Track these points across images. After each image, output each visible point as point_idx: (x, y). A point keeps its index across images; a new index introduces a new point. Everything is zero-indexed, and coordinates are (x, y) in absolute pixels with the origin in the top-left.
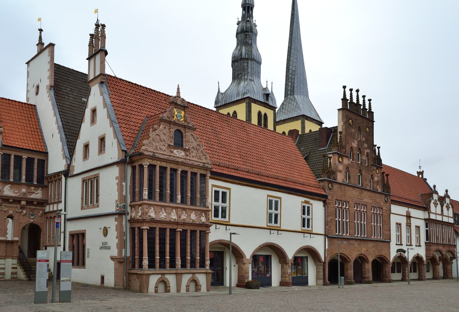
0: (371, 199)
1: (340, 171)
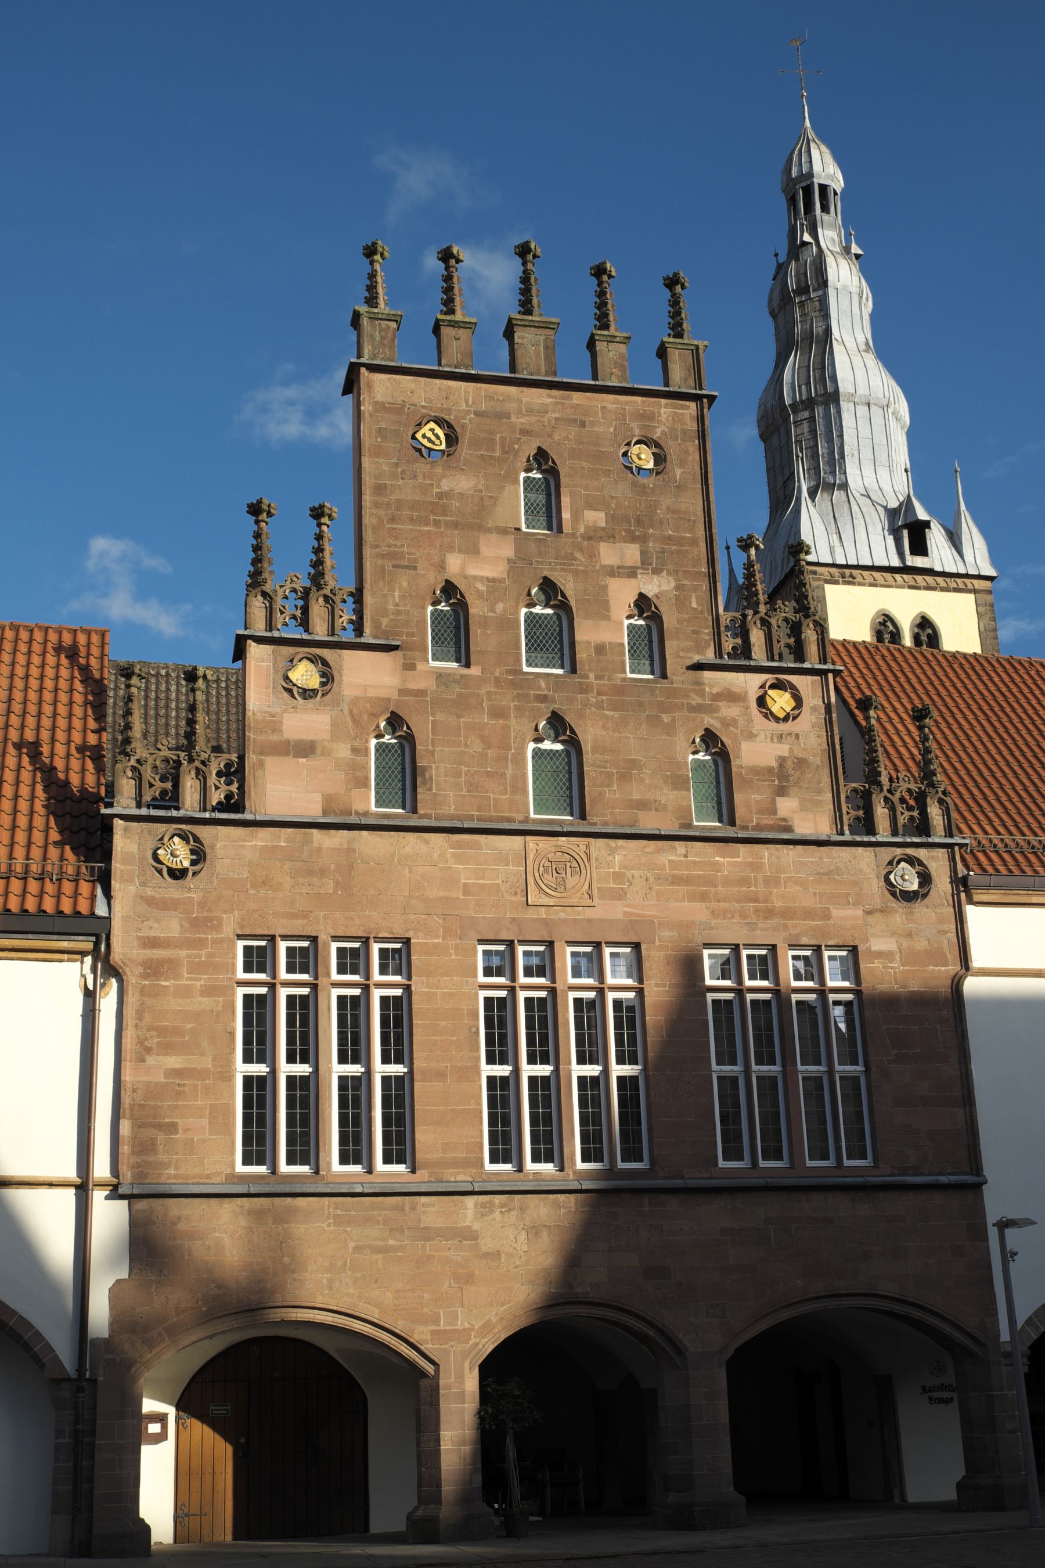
0: (704, 897)
1: (305, 749)
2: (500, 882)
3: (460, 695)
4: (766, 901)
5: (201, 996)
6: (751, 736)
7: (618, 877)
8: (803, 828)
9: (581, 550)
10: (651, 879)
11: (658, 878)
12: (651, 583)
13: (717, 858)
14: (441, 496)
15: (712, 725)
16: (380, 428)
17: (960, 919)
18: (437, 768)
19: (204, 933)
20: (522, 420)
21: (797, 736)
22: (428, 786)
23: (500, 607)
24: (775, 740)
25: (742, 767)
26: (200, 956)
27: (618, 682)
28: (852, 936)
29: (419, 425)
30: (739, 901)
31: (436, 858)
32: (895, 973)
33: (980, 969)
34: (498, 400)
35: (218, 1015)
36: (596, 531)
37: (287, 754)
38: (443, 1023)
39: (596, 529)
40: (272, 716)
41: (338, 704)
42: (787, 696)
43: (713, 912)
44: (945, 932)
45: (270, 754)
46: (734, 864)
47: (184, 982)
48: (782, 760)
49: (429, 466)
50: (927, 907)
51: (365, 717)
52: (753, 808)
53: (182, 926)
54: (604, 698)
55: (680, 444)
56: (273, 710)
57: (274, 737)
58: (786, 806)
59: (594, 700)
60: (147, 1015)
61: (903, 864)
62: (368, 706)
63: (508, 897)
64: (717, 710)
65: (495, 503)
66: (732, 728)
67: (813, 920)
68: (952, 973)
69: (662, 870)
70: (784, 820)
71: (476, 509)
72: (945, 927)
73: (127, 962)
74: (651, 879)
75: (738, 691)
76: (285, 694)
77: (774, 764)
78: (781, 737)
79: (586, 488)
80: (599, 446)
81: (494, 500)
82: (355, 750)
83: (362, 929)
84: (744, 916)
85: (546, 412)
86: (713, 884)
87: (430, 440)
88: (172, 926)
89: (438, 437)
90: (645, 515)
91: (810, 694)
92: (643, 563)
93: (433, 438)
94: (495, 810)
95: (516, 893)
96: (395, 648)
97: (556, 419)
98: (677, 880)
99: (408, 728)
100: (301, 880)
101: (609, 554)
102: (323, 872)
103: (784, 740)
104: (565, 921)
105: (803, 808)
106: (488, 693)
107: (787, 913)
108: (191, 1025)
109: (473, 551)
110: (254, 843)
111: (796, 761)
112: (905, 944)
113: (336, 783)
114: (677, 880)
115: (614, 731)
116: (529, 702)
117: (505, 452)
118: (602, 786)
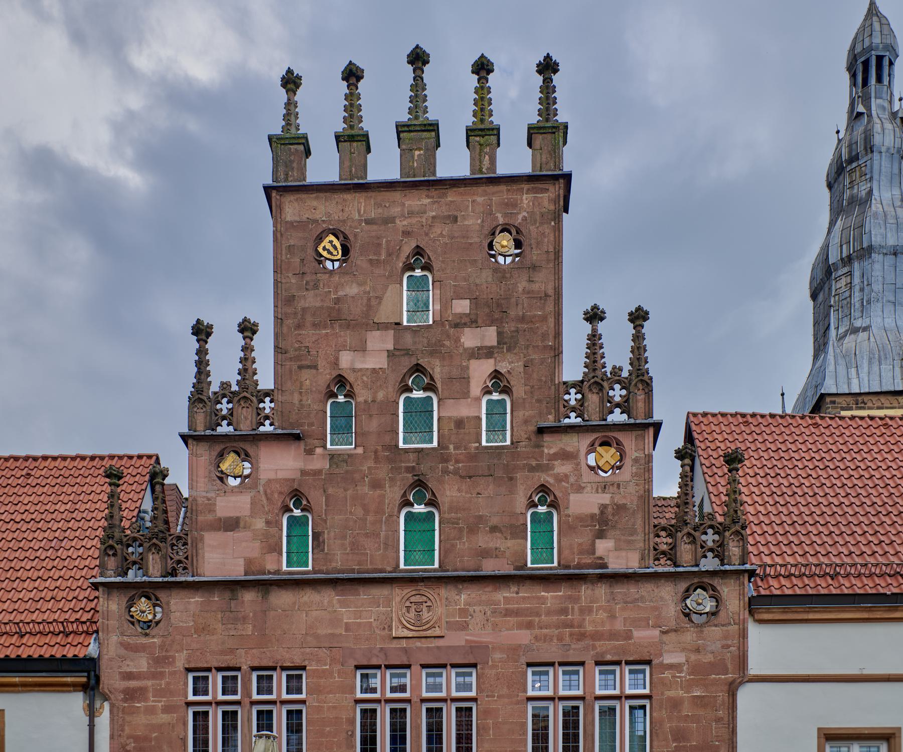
0: (529, 626)
1: (231, 525)
2: (372, 620)
3: (347, 472)
4: (580, 626)
5: (162, 713)
6: (580, 489)
7: (463, 612)
8: (615, 565)
9: (448, 337)
10: (489, 613)
11: (494, 612)
12: (504, 361)
13: (543, 594)
14: (338, 301)
15: (547, 482)
16: (289, 246)
17: (743, 635)
18: (329, 532)
19: (163, 667)
20: (405, 223)
21: (619, 486)
22: (321, 547)
23: (380, 395)
24: (600, 490)
25: (569, 516)
26: (161, 685)
27: (473, 450)
28: (648, 652)
29: (320, 239)
30: (557, 627)
31: (326, 604)
32: (681, 681)
33: (754, 676)
34: (385, 206)
35: (173, 727)
36: (461, 318)
37: (219, 530)
38: (328, 729)
39: (461, 316)
40: (209, 499)
41: (256, 487)
42: (613, 450)
43: (536, 638)
44: (728, 646)
45: (208, 531)
46: (556, 597)
47: (151, 704)
48: (603, 508)
49: (327, 275)
50: (716, 626)
51: (276, 495)
52: (575, 550)
53: (148, 664)
54: (460, 465)
55: (538, 227)
56: (209, 495)
57: (210, 517)
58: (603, 547)
59: (452, 467)
60: (126, 728)
61: (699, 591)
62: (278, 486)
63: (378, 632)
64: (552, 468)
65: (380, 303)
66: (564, 484)
67: (618, 640)
68: (730, 680)
69: (498, 605)
70: (601, 558)
71: (365, 309)
72: (730, 642)
73: (113, 690)
74: (489, 613)
75: (572, 450)
76: (218, 482)
77: (596, 511)
78: (605, 488)
79: (455, 279)
80: (468, 238)
81: (380, 299)
82: (268, 523)
83: (271, 661)
84: (560, 639)
85: (425, 212)
86: (538, 615)
87: (329, 252)
88: (142, 664)
89: (335, 248)
90: (504, 299)
91: (633, 447)
92: (499, 343)
93: (332, 250)
94: (371, 563)
95: (384, 629)
96: (297, 437)
97: (433, 217)
98: (508, 613)
99: (308, 502)
100: (230, 626)
101: (470, 339)
102: (245, 619)
103: (606, 491)
104: (420, 648)
105: (617, 548)
106: (369, 468)
107: (597, 636)
108: (156, 734)
109: (361, 348)
110: (197, 599)
111: (615, 507)
112: (693, 657)
113: (253, 549)
114: (508, 613)
115: (466, 492)
116: (400, 473)
117: (389, 255)
118: (454, 539)
